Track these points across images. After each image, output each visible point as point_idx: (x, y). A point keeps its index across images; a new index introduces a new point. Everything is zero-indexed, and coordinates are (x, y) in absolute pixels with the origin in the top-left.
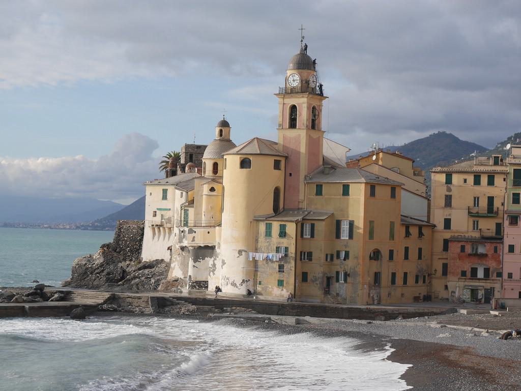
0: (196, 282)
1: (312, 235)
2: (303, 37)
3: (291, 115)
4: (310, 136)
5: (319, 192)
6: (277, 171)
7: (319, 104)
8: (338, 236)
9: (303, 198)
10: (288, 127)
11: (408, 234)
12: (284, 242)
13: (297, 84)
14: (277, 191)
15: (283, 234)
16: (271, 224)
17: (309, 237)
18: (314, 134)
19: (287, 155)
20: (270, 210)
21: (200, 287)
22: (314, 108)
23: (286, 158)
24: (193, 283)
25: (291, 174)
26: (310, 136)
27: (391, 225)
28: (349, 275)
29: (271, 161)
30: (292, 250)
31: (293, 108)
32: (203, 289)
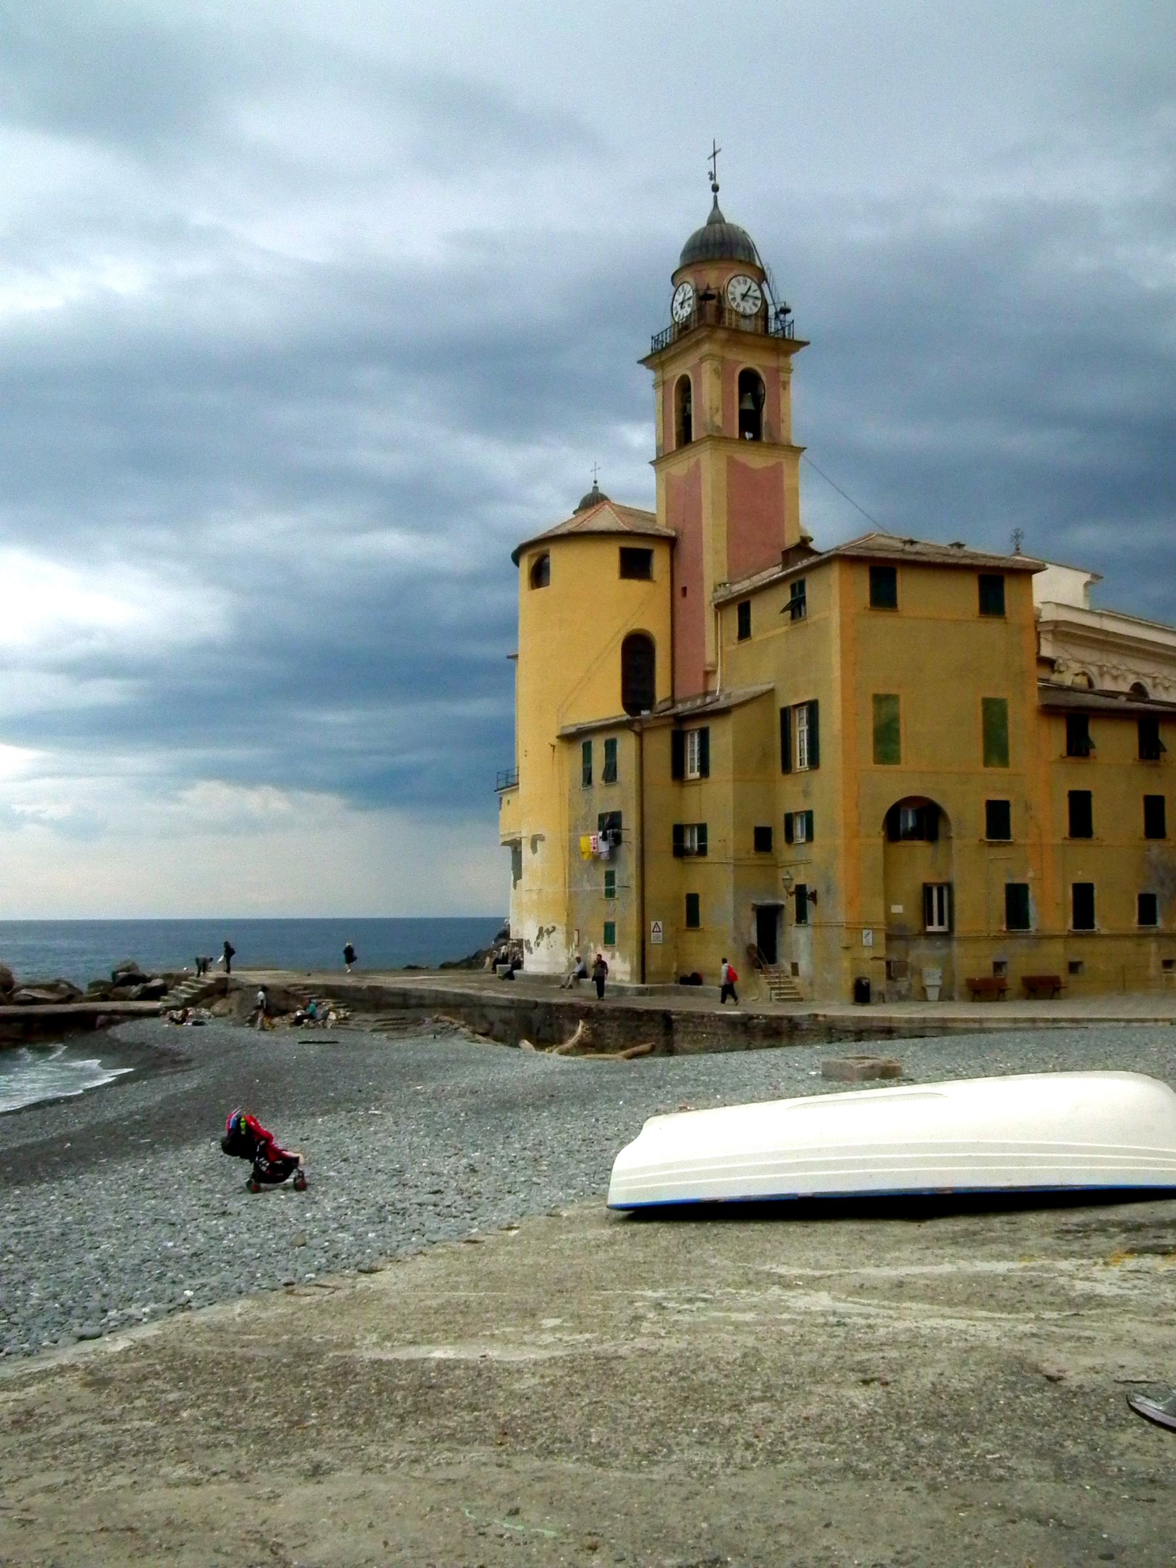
1: (704, 770)
4: (732, 463)
6: (635, 586)
8: (787, 766)
9: (714, 655)
11: (1078, 746)
16: (590, 743)
17: (697, 774)
18: (756, 460)
19: (673, 534)
23: (672, 542)
25: (684, 590)
27: (986, 711)
28: (814, 896)
29: (609, 557)
31: (684, 387)
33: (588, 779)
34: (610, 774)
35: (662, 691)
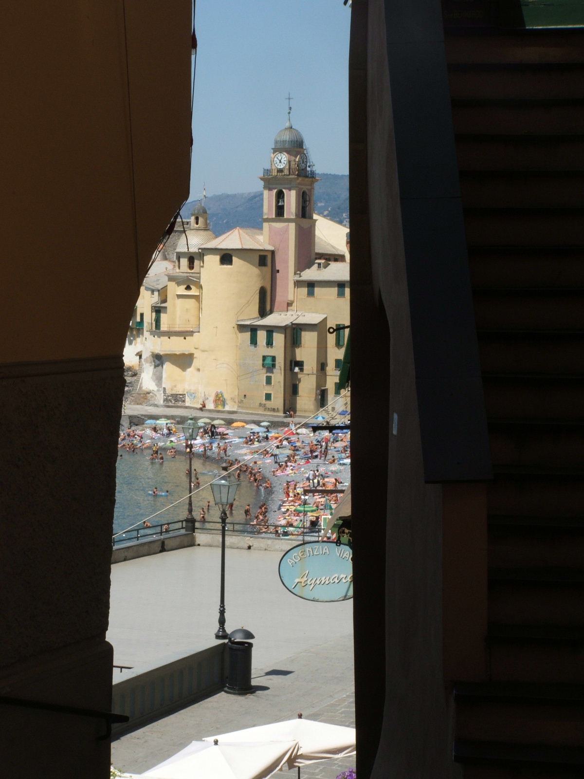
0: (172, 395)
2: (290, 108)
3: (277, 202)
5: (311, 294)
7: (309, 187)
10: (274, 216)
12: (270, 352)
13: (284, 165)
14: (262, 292)
15: (270, 343)
18: (305, 223)
19: (272, 248)
20: (256, 314)
21: (176, 400)
22: (304, 193)
24: (168, 396)
26: (300, 225)
30: (280, 362)
32: (180, 403)
33: (254, 341)
34: (270, 343)
35: (268, 308)
